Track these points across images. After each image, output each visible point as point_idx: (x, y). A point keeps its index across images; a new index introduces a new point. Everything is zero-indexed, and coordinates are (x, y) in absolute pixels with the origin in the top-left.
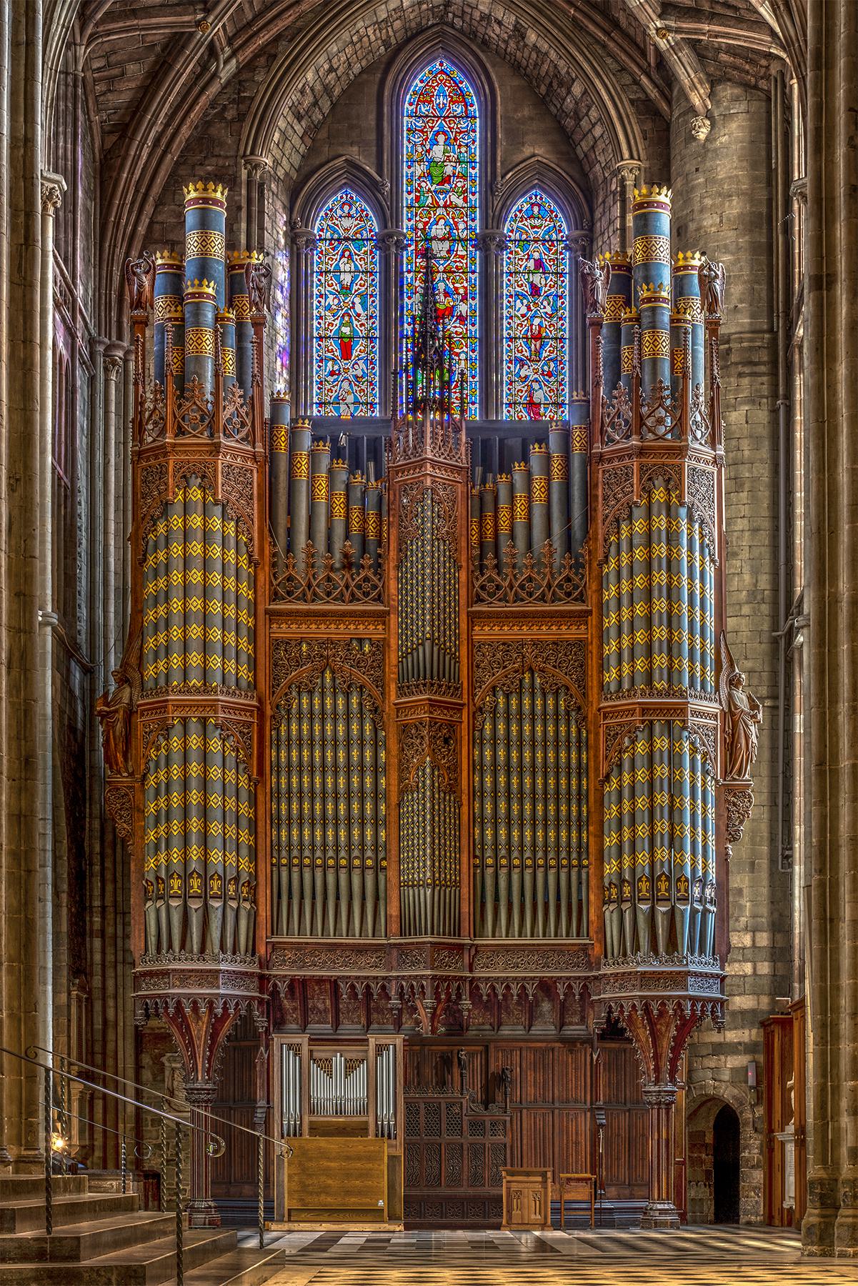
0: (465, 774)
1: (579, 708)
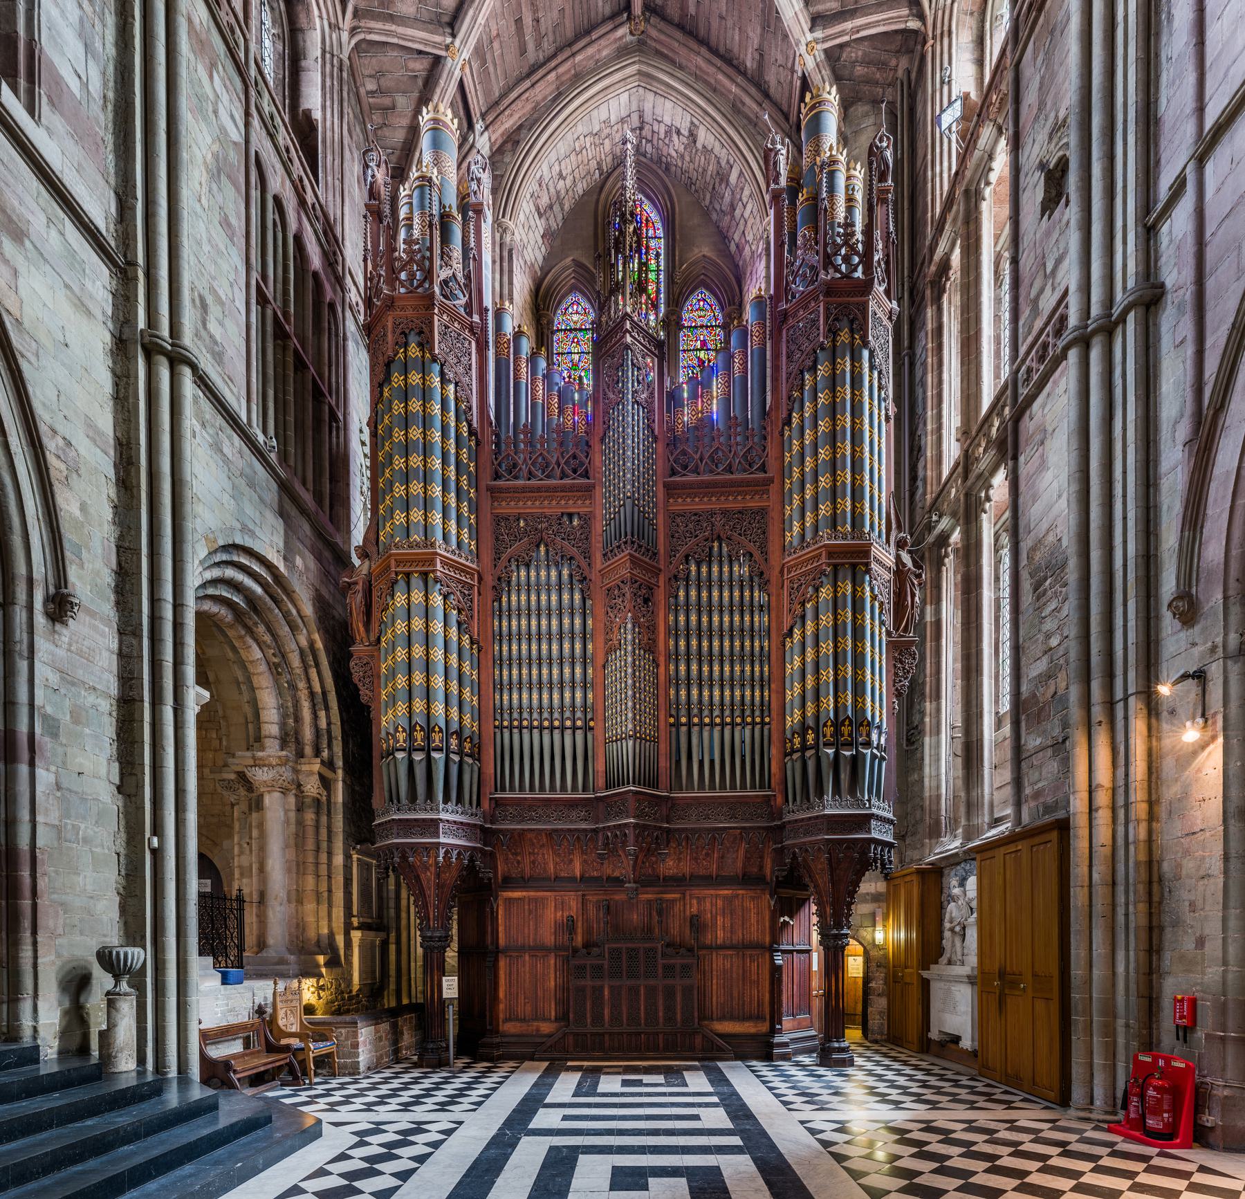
0: (662, 636)
1: (762, 573)
